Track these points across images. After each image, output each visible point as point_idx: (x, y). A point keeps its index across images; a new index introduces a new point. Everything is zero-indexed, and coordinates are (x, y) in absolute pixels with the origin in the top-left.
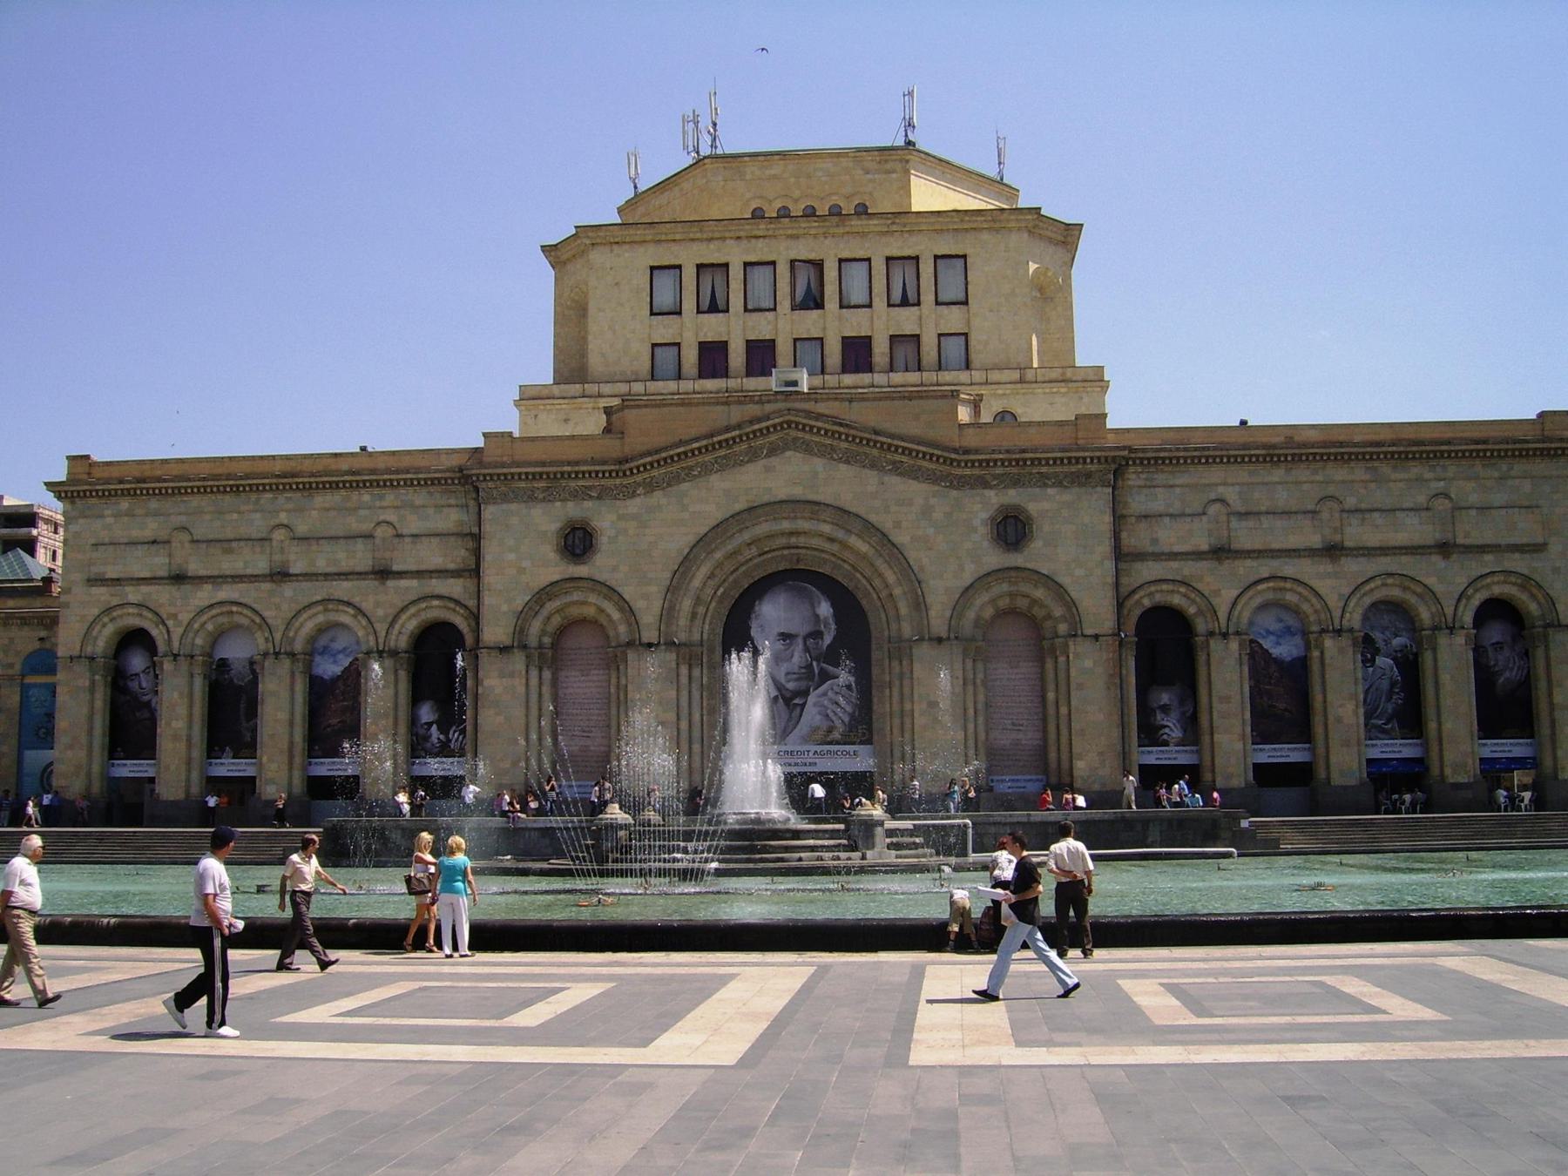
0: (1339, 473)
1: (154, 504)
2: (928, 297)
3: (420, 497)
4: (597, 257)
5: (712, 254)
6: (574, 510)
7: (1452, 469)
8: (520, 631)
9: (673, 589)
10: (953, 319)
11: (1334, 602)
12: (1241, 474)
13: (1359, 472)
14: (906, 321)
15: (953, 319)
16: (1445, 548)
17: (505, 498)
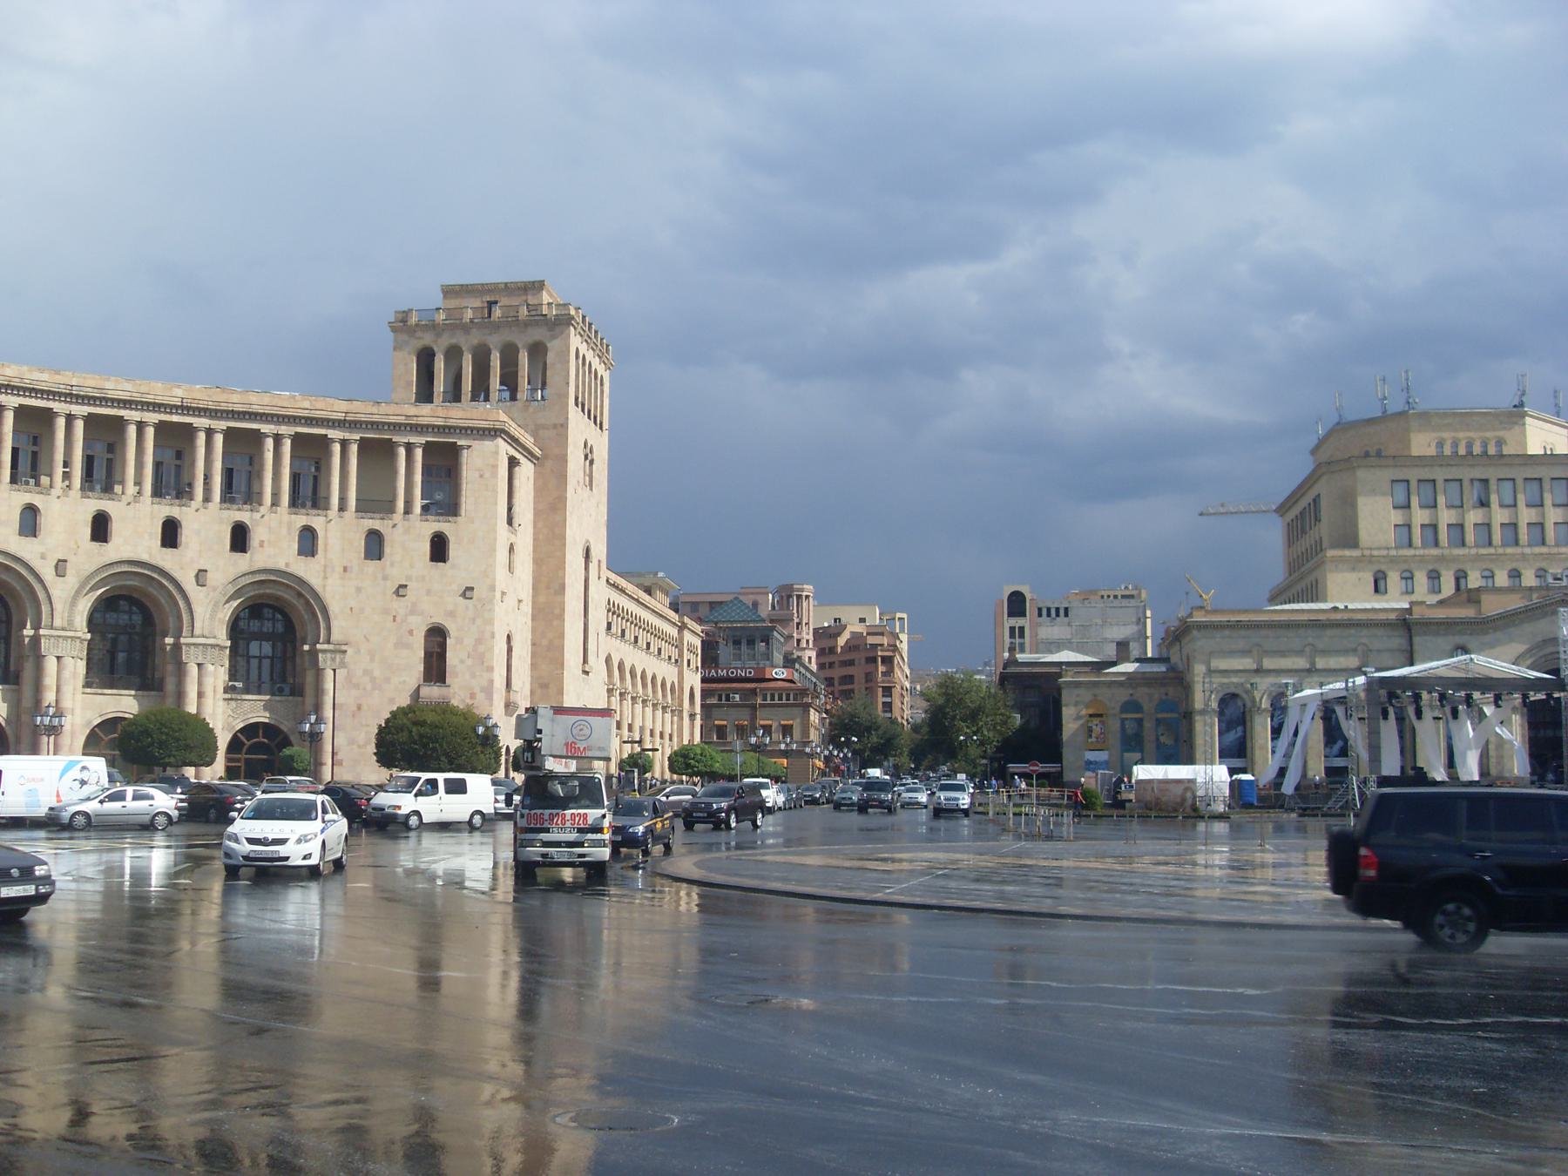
1: (1243, 632)
3: (1379, 632)
5: (1426, 474)
6: (1460, 640)
17: (1425, 634)
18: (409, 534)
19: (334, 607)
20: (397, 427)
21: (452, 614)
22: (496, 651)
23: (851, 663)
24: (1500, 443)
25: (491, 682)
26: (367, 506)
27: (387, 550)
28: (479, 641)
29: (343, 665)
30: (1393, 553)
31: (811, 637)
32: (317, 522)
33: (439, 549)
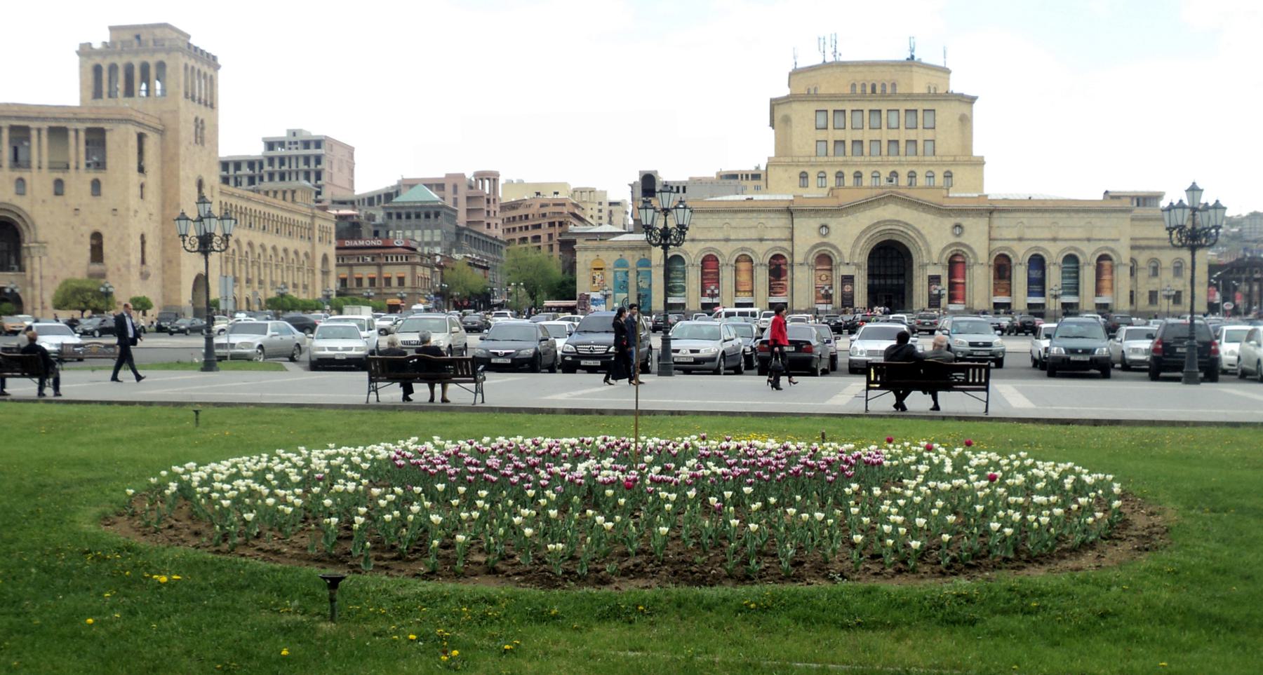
0: (1059, 215)
2: (920, 126)
3: (772, 215)
4: (795, 106)
5: (839, 106)
6: (823, 221)
7: (1093, 215)
8: (806, 259)
9: (854, 246)
10: (929, 134)
11: (1054, 255)
12: (1029, 215)
13: (1064, 215)
14: (912, 135)
15: (929, 134)
16: (1089, 240)
18: (78, 181)
19: (39, 222)
20: (69, 120)
21: (105, 225)
22: (132, 244)
23: (539, 226)
24: (894, 85)
25: (129, 261)
26: (53, 167)
27: (67, 190)
28: (121, 239)
29: (46, 255)
30: (813, 159)
31: (498, 209)
32: (26, 175)
33: (96, 186)
